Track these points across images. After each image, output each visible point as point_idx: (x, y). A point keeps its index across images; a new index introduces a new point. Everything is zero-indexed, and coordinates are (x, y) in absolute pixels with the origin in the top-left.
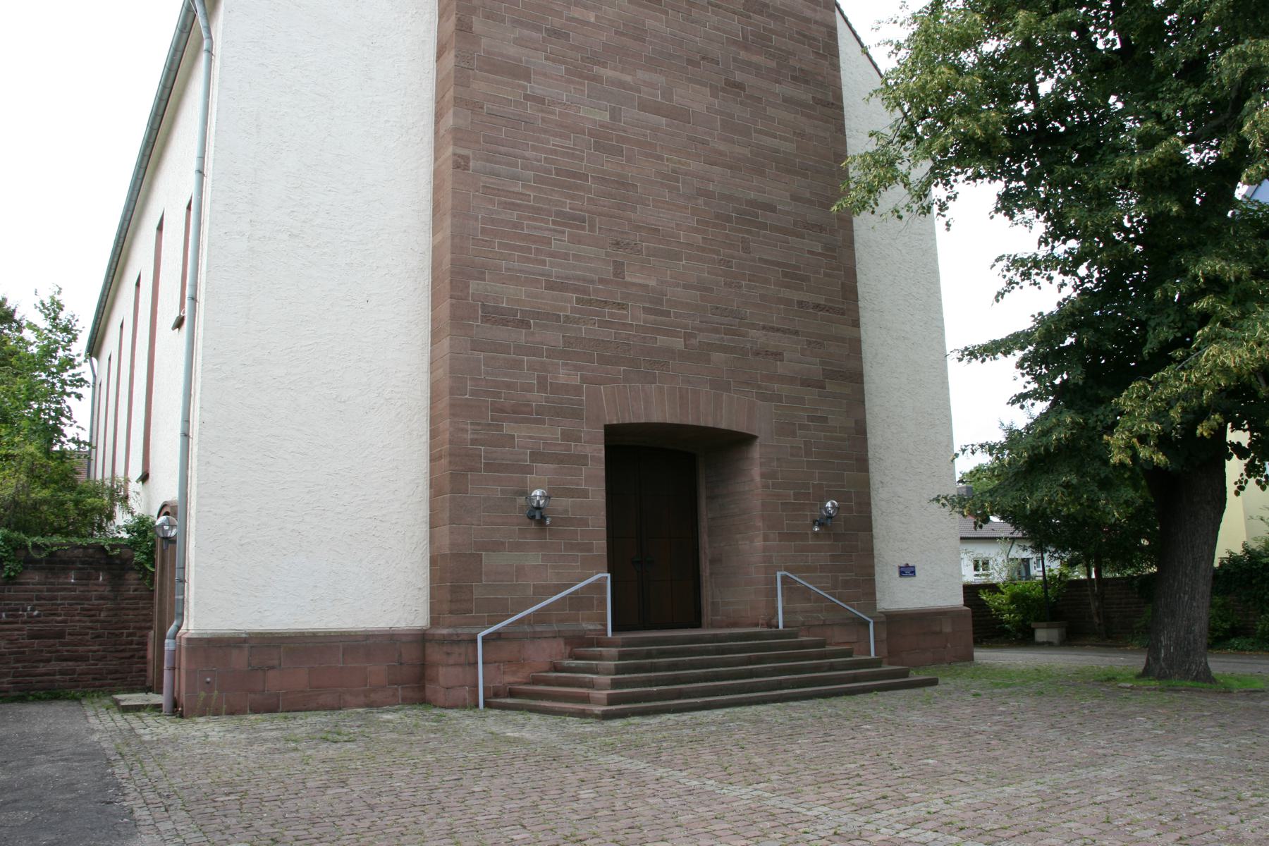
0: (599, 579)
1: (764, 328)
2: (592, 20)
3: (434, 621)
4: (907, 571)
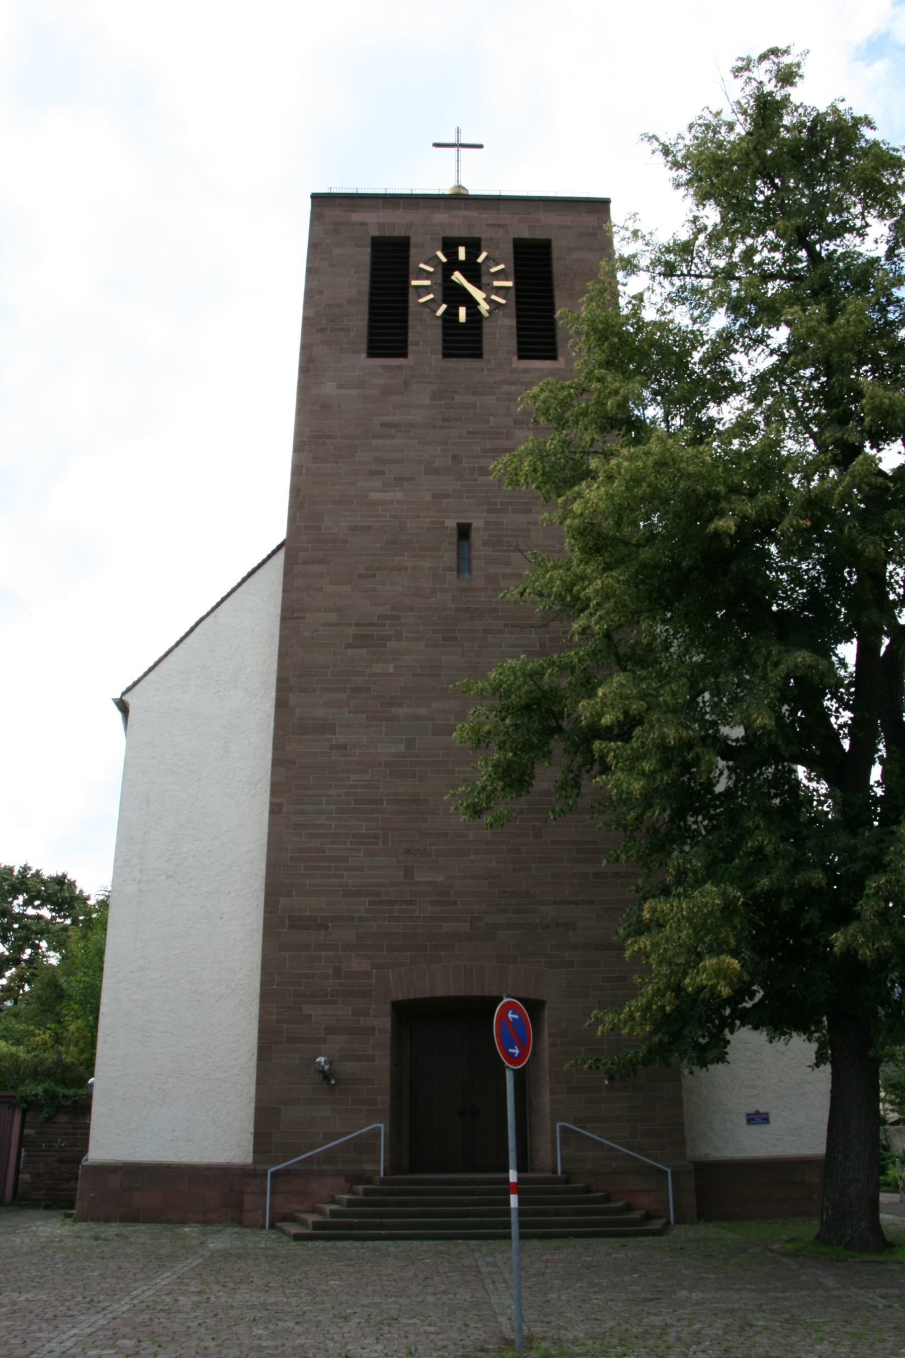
0: (375, 1128)
1: (555, 902)
2: (391, 670)
3: (255, 1161)
4: (758, 1118)
